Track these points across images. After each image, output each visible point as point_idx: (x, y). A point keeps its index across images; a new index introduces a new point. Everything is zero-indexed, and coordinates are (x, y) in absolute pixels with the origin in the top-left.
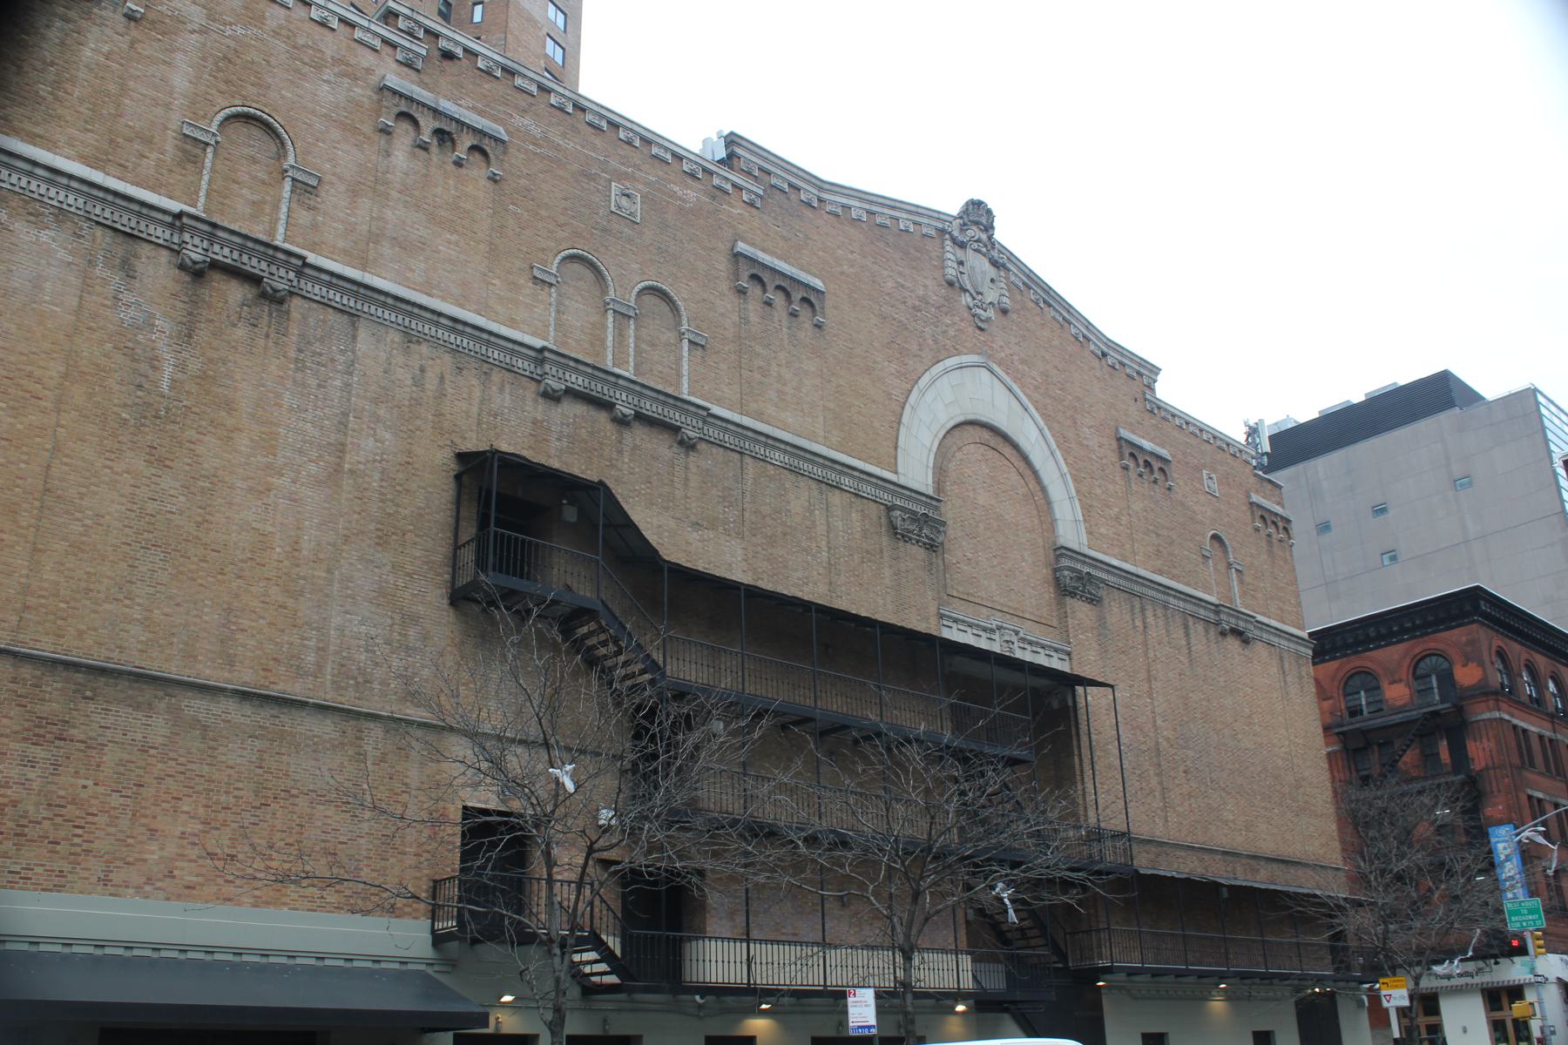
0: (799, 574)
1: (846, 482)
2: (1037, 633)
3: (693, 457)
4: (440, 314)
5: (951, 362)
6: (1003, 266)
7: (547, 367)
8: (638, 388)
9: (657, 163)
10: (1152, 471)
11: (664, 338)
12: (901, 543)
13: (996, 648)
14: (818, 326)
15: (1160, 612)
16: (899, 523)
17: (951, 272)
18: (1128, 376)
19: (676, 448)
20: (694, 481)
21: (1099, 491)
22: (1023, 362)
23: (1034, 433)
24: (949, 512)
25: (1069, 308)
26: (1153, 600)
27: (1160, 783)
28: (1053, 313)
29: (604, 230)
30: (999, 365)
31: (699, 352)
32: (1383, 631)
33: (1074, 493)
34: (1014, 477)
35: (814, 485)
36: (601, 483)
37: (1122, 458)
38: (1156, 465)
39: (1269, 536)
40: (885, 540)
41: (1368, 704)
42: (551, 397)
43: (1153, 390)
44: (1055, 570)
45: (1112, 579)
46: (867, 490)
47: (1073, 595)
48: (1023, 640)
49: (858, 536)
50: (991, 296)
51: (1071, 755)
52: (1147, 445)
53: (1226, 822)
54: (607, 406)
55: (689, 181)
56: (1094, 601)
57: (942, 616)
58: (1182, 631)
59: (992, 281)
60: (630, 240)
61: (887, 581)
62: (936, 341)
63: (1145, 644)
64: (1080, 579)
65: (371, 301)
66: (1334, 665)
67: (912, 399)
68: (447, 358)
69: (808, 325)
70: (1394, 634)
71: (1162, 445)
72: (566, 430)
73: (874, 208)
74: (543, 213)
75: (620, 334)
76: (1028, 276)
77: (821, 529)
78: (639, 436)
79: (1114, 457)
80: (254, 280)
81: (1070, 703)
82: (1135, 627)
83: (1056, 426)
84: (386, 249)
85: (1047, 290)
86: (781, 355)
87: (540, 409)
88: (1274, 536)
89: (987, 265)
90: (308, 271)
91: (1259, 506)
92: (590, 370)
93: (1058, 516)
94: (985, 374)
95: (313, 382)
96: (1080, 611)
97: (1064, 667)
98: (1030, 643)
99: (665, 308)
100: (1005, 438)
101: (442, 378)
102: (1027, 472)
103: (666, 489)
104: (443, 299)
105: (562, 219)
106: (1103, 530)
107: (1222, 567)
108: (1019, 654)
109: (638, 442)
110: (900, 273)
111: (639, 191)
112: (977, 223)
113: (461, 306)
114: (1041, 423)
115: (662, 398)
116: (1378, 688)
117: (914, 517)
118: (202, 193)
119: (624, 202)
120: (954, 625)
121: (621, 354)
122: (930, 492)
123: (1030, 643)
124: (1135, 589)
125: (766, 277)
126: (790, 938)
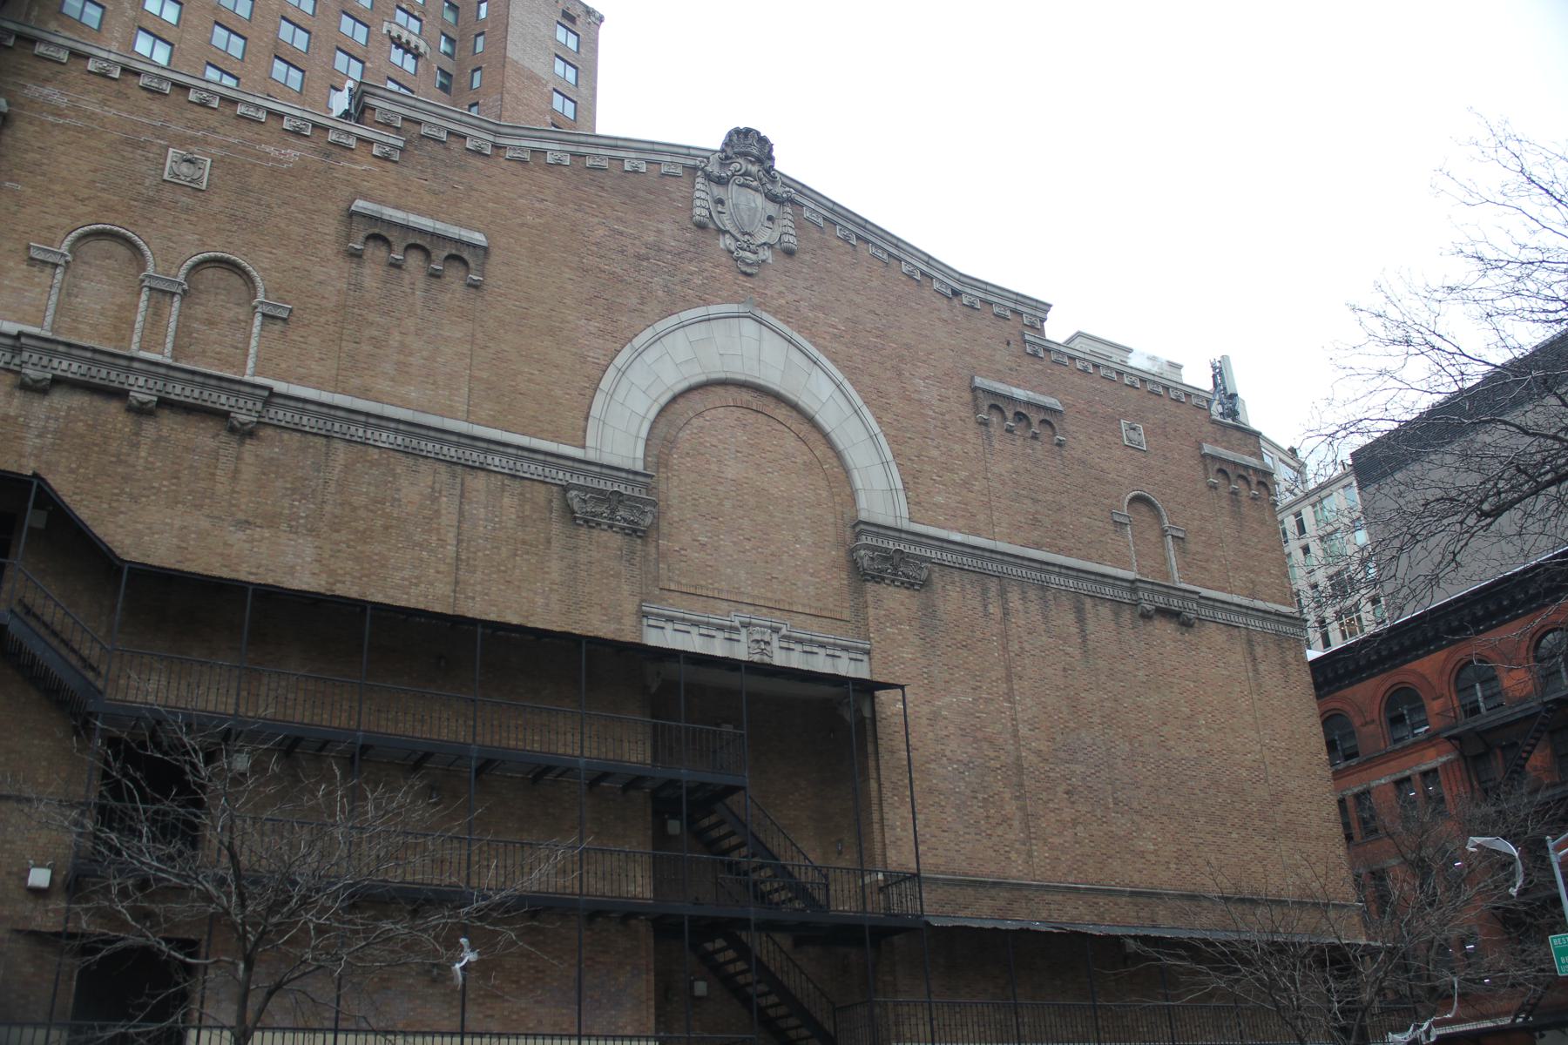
0: (406, 574)
1: (495, 461)
2: (816, 630)
3: (249, 447)
5: (686, 315)
6: (792, 201)
7: (25, 355)
8: (162, 371)
9: (243, 124)
10: (1029, 425)
11: (229, 315)
12: (583, 530)
13: (741, 651)
14: (475, 286)
15: (1032, 594)
16: (576, 505)
17: (700, 212)
18: (997, 316)
20: (248, 472)
21: (935, 453)
22: (813, 308)
23: (825, 389)
24: (676, 490)
25: (897, 243)
26: (1021, 581)
27: (1022, 809)
28: (872, 250)
29: (150, 201)
30: (775, 314)
31: (279, 326)
32: (1492, 607)
33: (889, 457)
34: (791, 443)
35: (442, 468)
36: (35, 475)
37: (977, 410)
38: (1035, 417)
39: (1235, 493)
40: (556, 528)
41: (1485, 698)
43: (1041, 331)
44: (852, 551)
45: (948, 557)
46: (529, 469)
47: (878, 579)
48: (787, 638)
50: (764, 236)
51: (867, 780)
52: (1020, 393)
53: (1142, 854)
54: (120, 394)
55: (292, 140)
56: (917, 585)
57: (646, 615)
58: (1071, 617)
59: (770, 218)
60: (187, 210)
61: (555, 576)
62: (669, 292)
63: (1005, 635)
66: (1440, 656)
67: (620, 361)
69: (458, 286)
70: (1506, 610)
71: (1051, 394)
72: (52, 425)
73: (583, 150)
74: (57, 188)
75: (156, 314)
76: (831, 211)
77: (448, 517)
78: (169, 424)
79: (966, 413)
81: (867, 713)
82: (987, 615)
83: (866, 379)
85: (864, 224)
86: (410, 323)
87: (16, 405)
88: (1244, 493)
89: (759, 200)
91: (1213, 458)
92: (89, 355)
93: (859, 484)
94: (749, 326)
96: (893, 599)
97: (860, 671)
98: (800, 641)
99: (236, 281)
100: (778, 398)
102: (813, 436)
103: (203, 484)
105: (86, 193)
106: (940, 499)
107: (1153, 535)
108: (779, 659)
109: (165, 432)
110: (619, 219)
111: (211, 156)
112: (744, 155)
114: (839, 376)
115: (198, 379)
116: (1494, 678)
117: (602, 497)
119: (185, 168)
120: (669, 626)
121: (152, 340)
122: (639, 467)
123: (800, 641)
124: (985, 569)
125: (392, 236)
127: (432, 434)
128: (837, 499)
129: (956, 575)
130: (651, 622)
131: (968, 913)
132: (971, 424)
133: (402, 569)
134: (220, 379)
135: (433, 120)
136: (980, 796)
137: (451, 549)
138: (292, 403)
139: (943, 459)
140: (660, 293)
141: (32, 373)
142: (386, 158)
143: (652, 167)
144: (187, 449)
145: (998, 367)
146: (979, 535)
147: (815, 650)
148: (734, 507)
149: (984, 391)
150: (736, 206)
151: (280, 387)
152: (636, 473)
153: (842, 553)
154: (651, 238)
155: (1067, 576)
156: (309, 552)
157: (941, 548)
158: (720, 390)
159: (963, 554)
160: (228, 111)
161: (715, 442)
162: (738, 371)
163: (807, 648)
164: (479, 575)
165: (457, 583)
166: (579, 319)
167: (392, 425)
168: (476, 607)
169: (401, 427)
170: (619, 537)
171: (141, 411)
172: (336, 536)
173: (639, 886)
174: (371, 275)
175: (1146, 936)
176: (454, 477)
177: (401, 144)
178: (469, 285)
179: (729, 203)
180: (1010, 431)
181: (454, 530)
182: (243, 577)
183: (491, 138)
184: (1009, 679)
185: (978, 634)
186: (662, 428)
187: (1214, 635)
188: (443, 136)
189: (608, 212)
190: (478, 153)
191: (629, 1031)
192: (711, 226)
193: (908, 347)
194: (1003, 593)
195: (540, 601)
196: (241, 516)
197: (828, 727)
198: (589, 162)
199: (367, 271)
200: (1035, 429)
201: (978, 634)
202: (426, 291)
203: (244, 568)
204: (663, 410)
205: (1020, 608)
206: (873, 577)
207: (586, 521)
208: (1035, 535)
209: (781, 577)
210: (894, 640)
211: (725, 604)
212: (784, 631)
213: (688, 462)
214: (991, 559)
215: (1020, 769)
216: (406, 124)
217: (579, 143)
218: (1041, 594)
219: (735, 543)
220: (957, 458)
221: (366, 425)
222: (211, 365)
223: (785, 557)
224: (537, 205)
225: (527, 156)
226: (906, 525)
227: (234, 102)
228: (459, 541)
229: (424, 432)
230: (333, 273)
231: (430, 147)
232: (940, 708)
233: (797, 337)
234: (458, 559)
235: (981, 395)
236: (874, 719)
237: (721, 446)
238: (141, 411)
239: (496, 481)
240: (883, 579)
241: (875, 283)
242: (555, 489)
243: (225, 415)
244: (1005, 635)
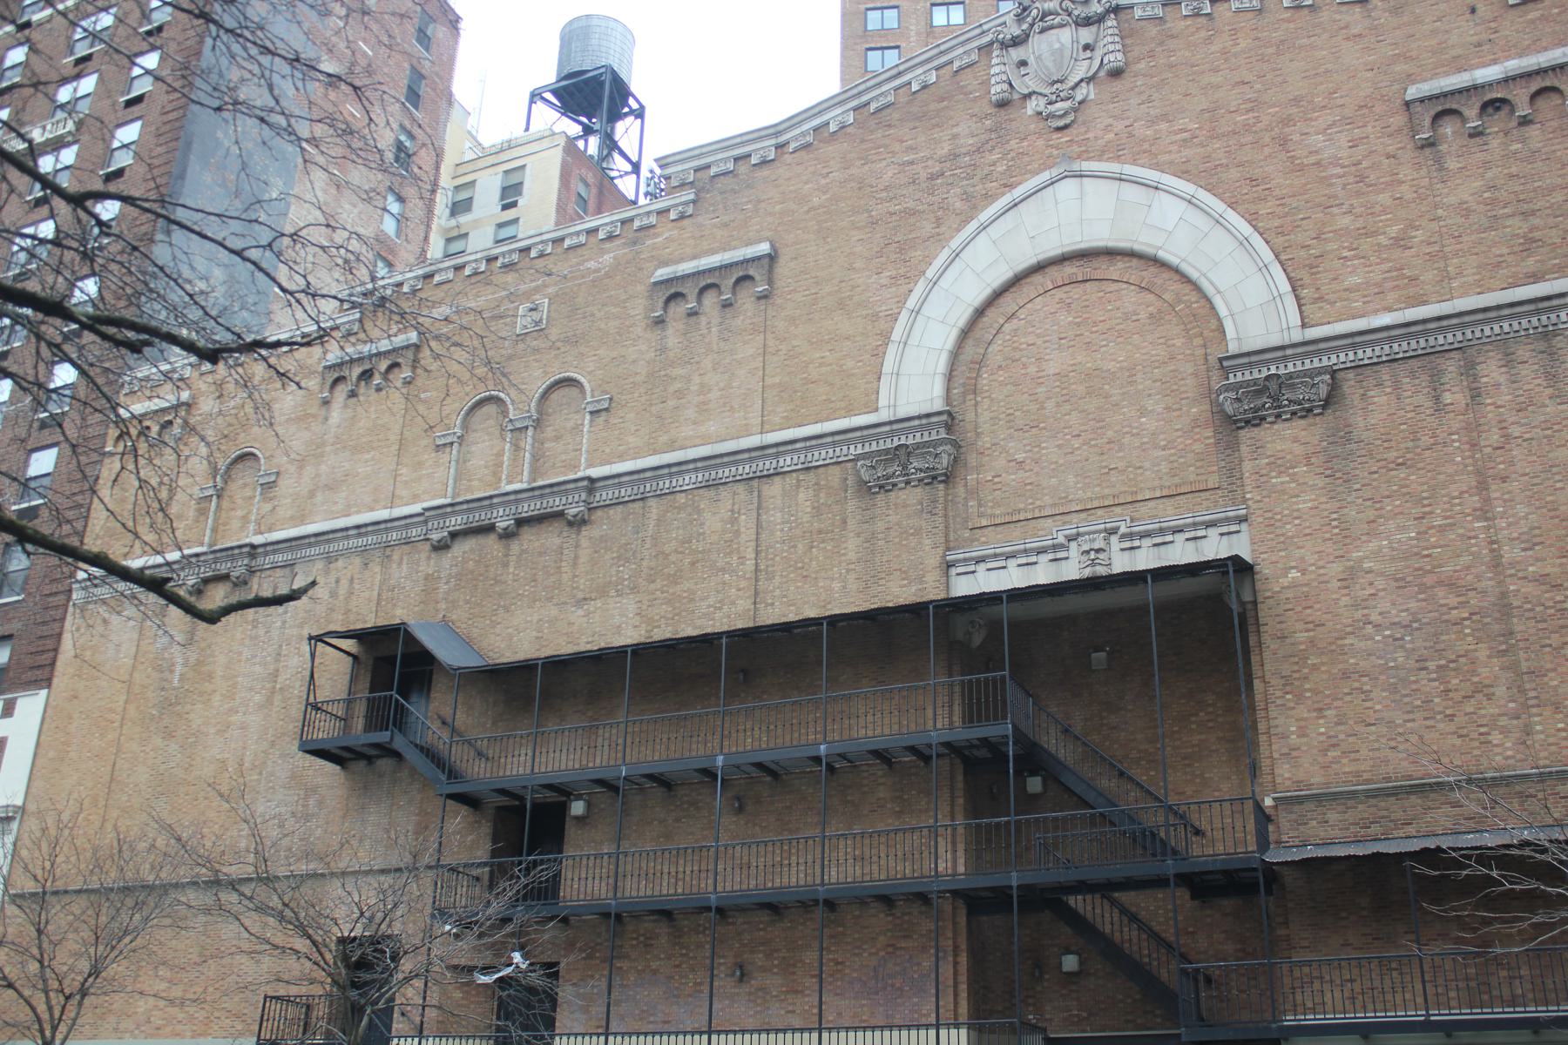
0: (711, 601)
2: (1171, 514)
3: (586, 532)
4: (347, 529)
5: (984, 216)
13: (1072, 570)
17: (997, 90)
19: (566, 531)
22: (1152, 122)
26: (1502, 341)
27: (1513, 667)
30: (1100, 158)
33: (1267, 254)
34: (1130, 299)
35: (740, 488)
40: (851, 505)
42: (441, 547)
46: (819, 456)
48: (1129, 536)
49: (806, 518)
54: (490, 528)
55: (608, 245)
59: (1087, 47)
61: (852, 556)
64: (1259, 393)
65: (300, 547)
68: (357, 561)
72: (454, 570)
73: (864, 99)
78: (531, 539)
80: (226, 577)
81: (1247, 597)
84: (319, 498)
86: (707, 363)
90: (260, 550)
93: (1222, 311)
94: (1068, 188)
95: (261, 631)
96: (1284, 439)
100: (1111, 253)
101: (352, 580)
103: (552, 579)
104: (358, 512)
108: (1121, 563)
113: (372, 510)
114: (1188, 188)
115: (537, 493)
118: (208, 532)
124: (1427, 349)
126: (659, 1028)
127: (726, 459)
128: (1199, 341)
129: (1385, 373)
130: (960, 570)
131: (1411, 830)
132: (1408, 154)
133: (707, 598)
134: (551, 486)
135: (720, 156)
136: (1431, 665)
137: (750, 564)
138: (610, 482)
139: (1360, 223)
140: (958, 205)
141: (435, 536)
142: (682, 217)
143: (942, 72)
144: (541, 554)
145: (1454, 53)
146: (1424, 303)
147: (1169, 538)
148: (1058, 405)
149: (1422, 100)
150: (1038, 58)
151: (595, 472)
152: (928, 416)
153: (1208, 407)
154: (944, 149)
156: (632, 608)
157: (1354, 346)
158: (1037, 278)
159: (1391, 339)
160: (559, 250)
161: (1031, 339)
162: (1052, 246)
163: (1159, 540)
164: (777, 580)
165: (756, 594)
166: (869, 277)
167: (691, 466)
168: (776, 613)
169: (699, 464)
170: (919, 490)
171: (507, 535)
172: (652, 586)
173: (949, 862)
174: (673, 336)
175: (1425, 850)
176: (751, 492)
177: (692, 197)
178: (759, 298)
179: (1031, 60)
180: (1476, 134)
181: (753, 544)
182: (812, 613)
183: (773, 142)
184: (1482, 486)
185: (1426, 440)
186: (970, 351)
188: (730, 166)
189: (897, 147)
190: (764, 162)
191: (751, 1023)
192: (1016, 96)
193: (1296, 101)
194: (1469, 370)
195: (837, 585)
196: (580, 595)
197: (1196, 630)
198: (873, 106)
199: (670, 331)
200: (1523, 110)
201: (1426, 440)
202: (721, 324)
203: (584, 639)
204: (965, 334)
205: (1502, 379)
206: (1247, 422)
207: (881, 487)
208: (1531, 264)
209: (1121, 465)
210: (1283, 492)
211: (1050, 520)
212: (1123, 530)
213: (1001, 376)
214: (1441, 330)
215: (1505, 609)
216: (699, 174)
217: (860, 94)
218: (1542, 345)
219: (1059, 447)
220: (1384, 212)
221: (671, 475)
222: (557, 475)
223: (1126, 440)
224: (823, 182)
225: (809, 139)
226: (1297, 336)
227: (562, 239)
228: (757, 553)
229: (718, 461)
230: (644, 347)
231: (722, 183)
232: (1361, 560)
233: (1130, 170)
234: (757, 570)
235: (1418, 108)
236: (1255, 603)
237: (1039, 342)
238: (507, 535)
239: (790, 480)
240: (1263, 419)
241: (1243, 44)
242: (849, 465)
243: (560, 515)
244: (1473, 429)
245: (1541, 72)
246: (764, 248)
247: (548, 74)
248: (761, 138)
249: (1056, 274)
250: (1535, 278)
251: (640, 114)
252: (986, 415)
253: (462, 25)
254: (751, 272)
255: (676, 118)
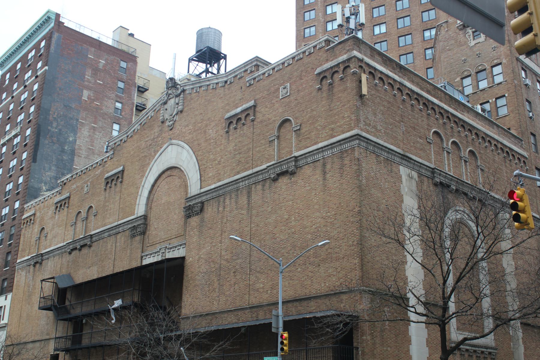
53: (258, 290)
123: (171, 248)
155: (245, 180)
168: (118, 270)
183: (126, 135)
187: (307, 171)
217: (140, 120)
238: (80, 250)
245: (331, 68)
246: (252, 103)
247: (192, 52)
248: (240, 69)
249: (164, 176)
250: (238, 173)
251: (225, 57)
252: (152, 215)
253: (138, 60)
254: (232, 120)
255: (235, 57)
